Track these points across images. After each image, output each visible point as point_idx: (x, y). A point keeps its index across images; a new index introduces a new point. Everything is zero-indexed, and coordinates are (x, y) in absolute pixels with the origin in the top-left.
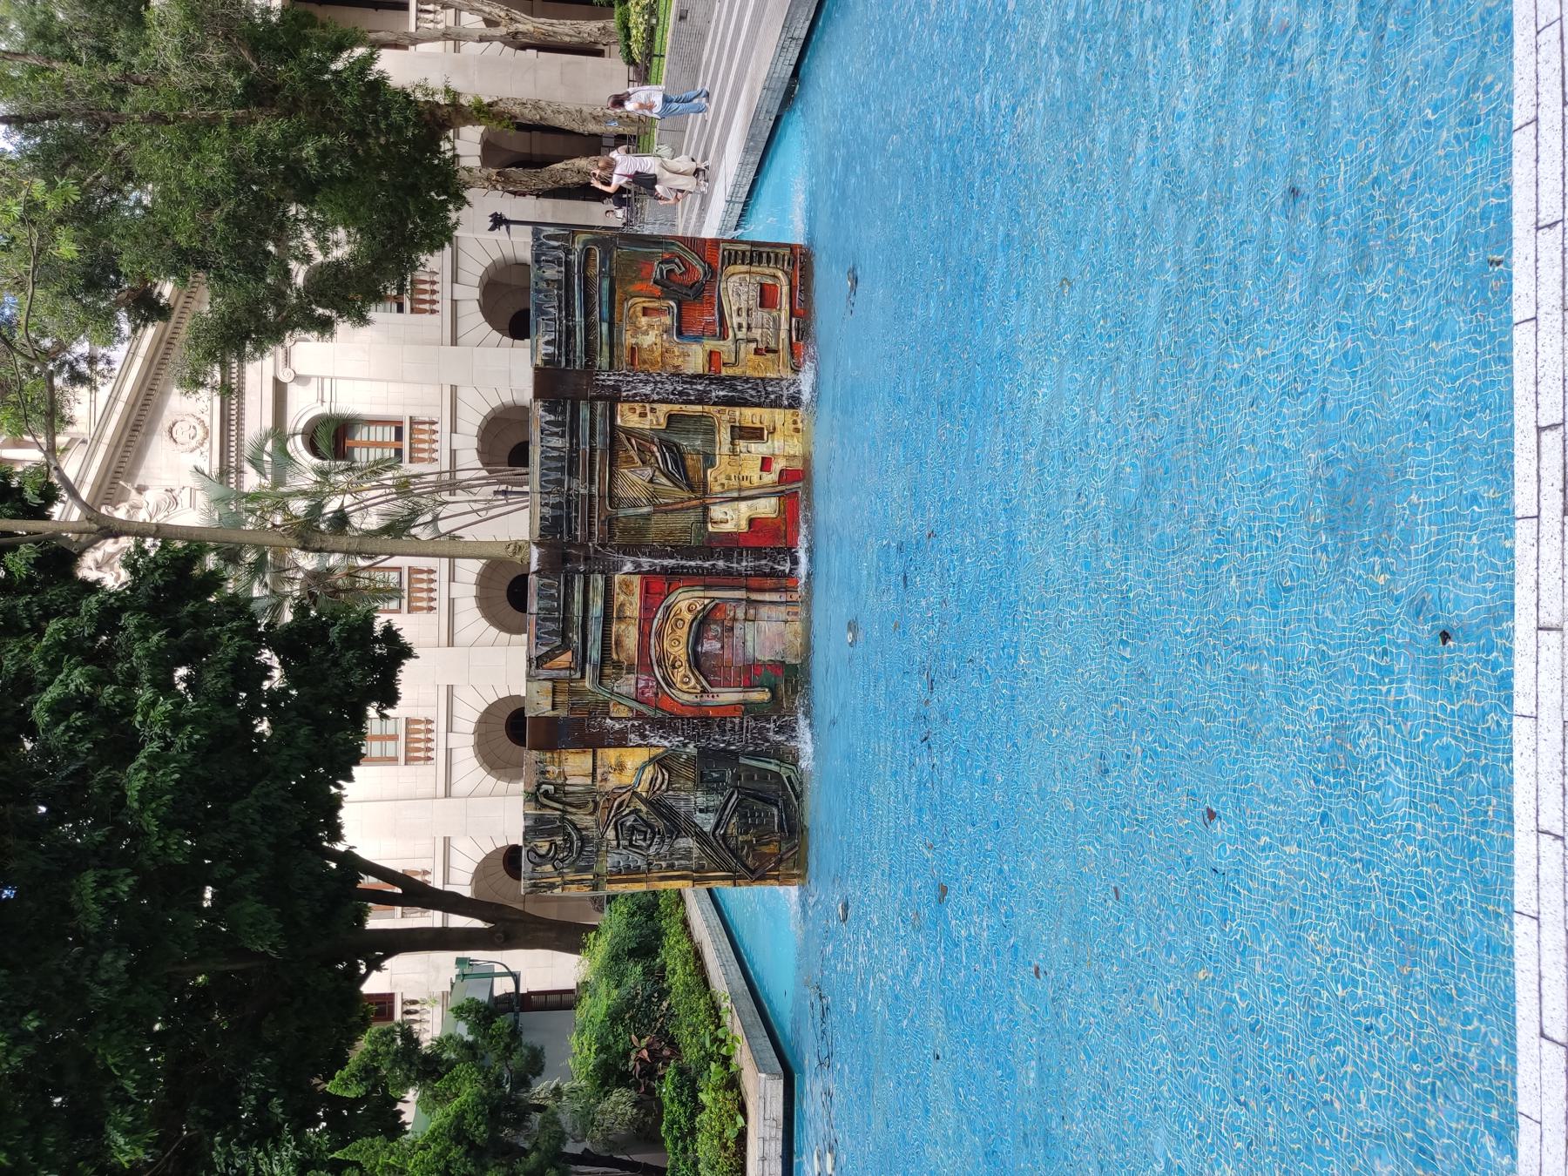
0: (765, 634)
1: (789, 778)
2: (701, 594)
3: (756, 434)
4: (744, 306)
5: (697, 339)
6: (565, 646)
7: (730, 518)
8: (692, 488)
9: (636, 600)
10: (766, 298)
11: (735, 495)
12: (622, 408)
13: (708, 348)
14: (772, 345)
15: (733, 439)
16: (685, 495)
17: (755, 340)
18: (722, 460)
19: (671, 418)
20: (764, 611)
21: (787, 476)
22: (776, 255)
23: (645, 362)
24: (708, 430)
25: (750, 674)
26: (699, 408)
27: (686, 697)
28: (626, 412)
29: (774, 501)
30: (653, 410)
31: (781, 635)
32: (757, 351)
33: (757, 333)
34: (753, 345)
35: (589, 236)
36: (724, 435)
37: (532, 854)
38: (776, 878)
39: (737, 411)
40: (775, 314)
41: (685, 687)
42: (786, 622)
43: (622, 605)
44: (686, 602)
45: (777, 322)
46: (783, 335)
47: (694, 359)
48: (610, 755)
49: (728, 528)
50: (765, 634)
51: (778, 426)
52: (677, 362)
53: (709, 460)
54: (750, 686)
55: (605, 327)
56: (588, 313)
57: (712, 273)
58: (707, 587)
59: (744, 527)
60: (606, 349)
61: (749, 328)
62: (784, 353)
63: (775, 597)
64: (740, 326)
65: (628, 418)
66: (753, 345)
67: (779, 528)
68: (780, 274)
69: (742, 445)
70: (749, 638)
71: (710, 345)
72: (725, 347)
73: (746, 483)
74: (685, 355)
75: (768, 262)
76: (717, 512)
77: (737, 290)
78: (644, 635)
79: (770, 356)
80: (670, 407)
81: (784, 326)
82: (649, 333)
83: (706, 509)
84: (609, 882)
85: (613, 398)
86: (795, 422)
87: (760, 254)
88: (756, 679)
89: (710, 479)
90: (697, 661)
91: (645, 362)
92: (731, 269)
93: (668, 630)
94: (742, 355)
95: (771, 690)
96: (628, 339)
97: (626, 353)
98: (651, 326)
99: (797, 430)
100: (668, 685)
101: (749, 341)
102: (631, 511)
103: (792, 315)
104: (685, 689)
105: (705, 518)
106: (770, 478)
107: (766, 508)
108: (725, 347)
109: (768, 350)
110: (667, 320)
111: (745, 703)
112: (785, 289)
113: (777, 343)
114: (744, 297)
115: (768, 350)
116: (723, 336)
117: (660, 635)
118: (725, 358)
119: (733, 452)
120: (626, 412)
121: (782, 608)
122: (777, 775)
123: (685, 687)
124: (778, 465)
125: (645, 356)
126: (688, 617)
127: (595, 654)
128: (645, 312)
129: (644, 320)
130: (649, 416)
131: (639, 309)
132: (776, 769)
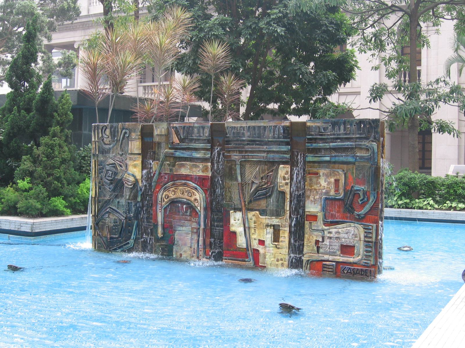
0: (186, 236)
1: (128, 243)
2: (202, 206)
3: (276, 238)
4: (342, 235)
5: (324, 209)
6: (182, 140)
7: (236, 222)
8: (250, 202)
9: (201, 174)
10: (347, 249)
11: (247, 225)
12: (288, 168)
13: (319, 214)
14: (321, 250)
15: (274, 226)
16: (247, 200)
17: (323, 241)
18: (265, 220)
19: (283, 193)
20: (195, 237)
21: (256, 252)
22: (370, 256)
23: (311, 180)
24: (278, 213)
25: (169, 228)
26: (288, 209)
27: (160, 197)
28: (285, 170)
29: (245, 246)
30: (287, 184)
31: (185, 245)
32: (317, 242)
33: (327, 242)
34: (321, 240)
35: (376, 151)
36: (275, 221)
37: (105, 128)
38: (95, 235)
39: (287, 229)
40: (338, 253)
41: (164, 196)
42: (191, 247)
43: (198, 167)
44: (198, 198)
45: (333, 254)
46: (326, 257)
47: (312, 207)
48: (139, 162)
49: (232, 221)
50: (186, 236)
51: (280, 251)
52: (311, 198)
53: (263, 212)
54: (164, 228)
55: (328, 159)
56: (335, 149)
57: (360, 219)
58: (205, 209)
59: (232, 229)
60: (316, 159)
61: (330, 238)
62: (316, 257)
63: (201, 243)
64: (330, 233)
65: (283, 171)
66: (321, 240)
67: (231, 247)
68: (360, 257)
69: (271, 230)
70: (184, 228)
71: (320, 215)
72: (319, 224)
73: (252, 231)
74: (315, 201)
75: (367, 251)
76: (239, 215)
77: (351, 232)
78: (187, 177)
79: (315, 248)
80: (289, 193)
81: (331, 258)
82: (324, 183)
83: (240, 210)
84: (95, 161)
85: (292, 162)
86: (282, 260)
87: (371, 247)
88: (167, 231)
89: (254, 213)
90: (173, 202)
91: (311, 180)
92: (361, 229)
93: (188, 189)
94: (316, 233)
95: (162, 238)
96: (322, 172)
97: (315, 170)
98: (329, 183)
99: (278, 260)
100: (165, 188)
101: (323, 238)
102: (238, 171)
103: (337, 263)
104: (164, 196)
105: (236, 210)
106: (255, 244)
107: (241, 242)
108: (319, 224)
109: (318, 248)
110: (332, 193)
111: (157, 225)
112: (351, 260)
113: (322, 253)
114: (346, 236)
115: (318, 248)
116: (326, 224)
117: (185, 184)
118: (314, 223)
119: (267, 226)
120: (285, 170)
121: (196, 246)
122: (129, 238)
123: (164, 196)
124: (261, 249)
125: (314, 180)
126: (192, 199)
127: (178, 154)
128: (337, 181)
129: (332, 180)
130: (283, 182)
131: (338, 177)
132: (132, 237)
